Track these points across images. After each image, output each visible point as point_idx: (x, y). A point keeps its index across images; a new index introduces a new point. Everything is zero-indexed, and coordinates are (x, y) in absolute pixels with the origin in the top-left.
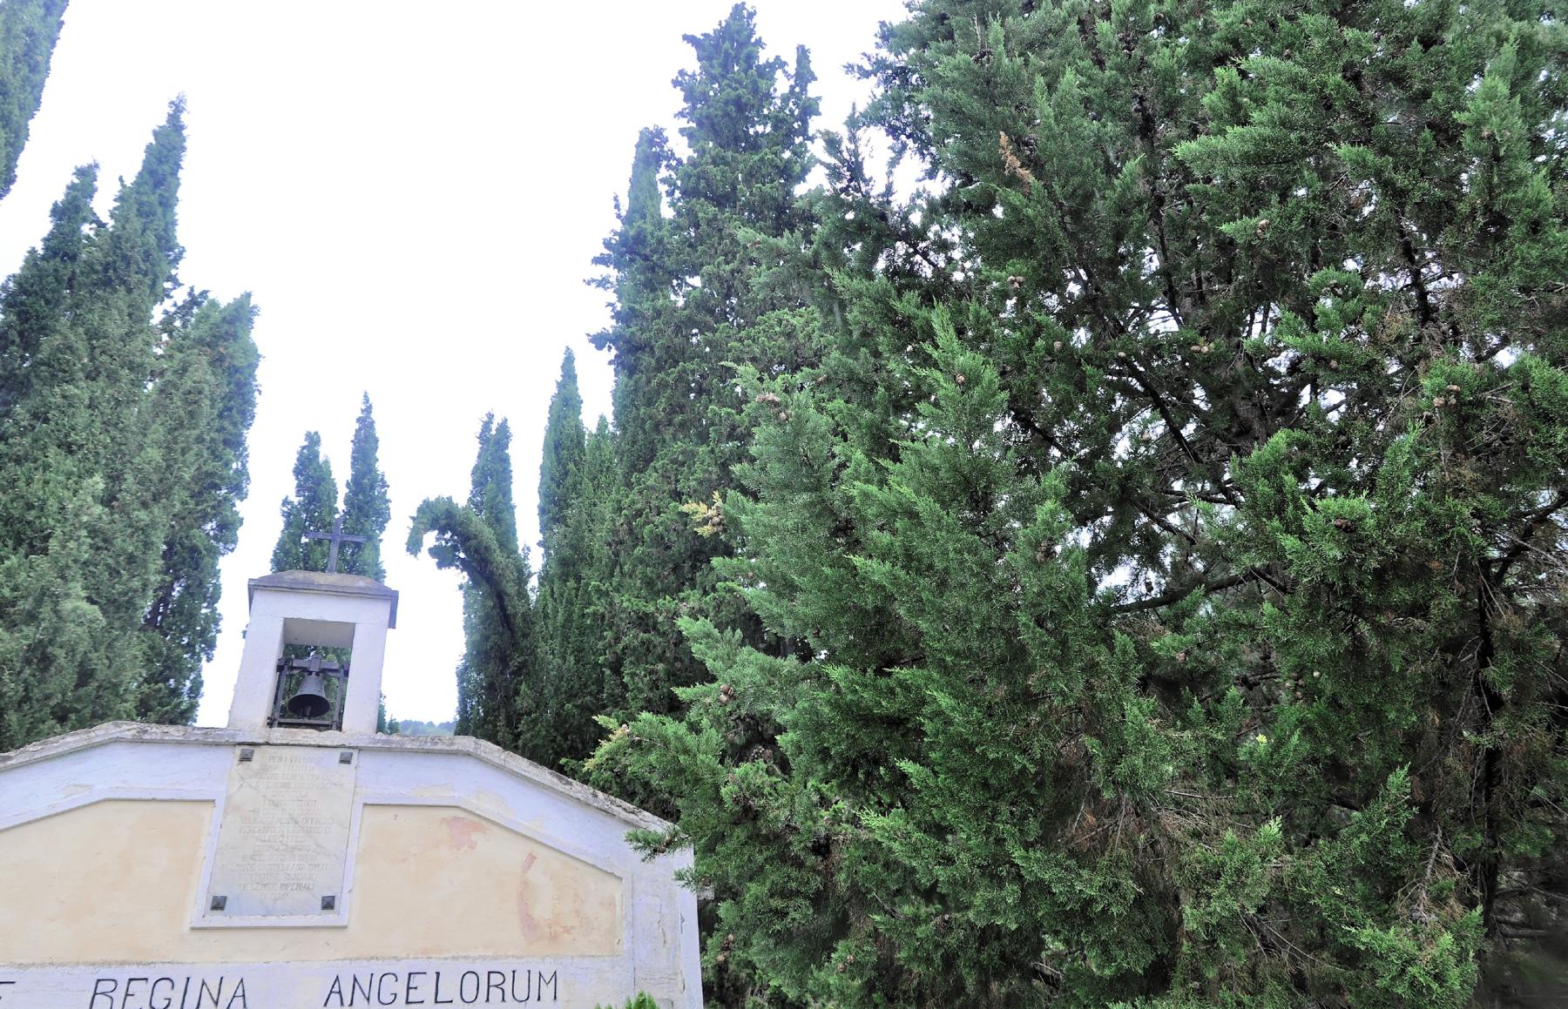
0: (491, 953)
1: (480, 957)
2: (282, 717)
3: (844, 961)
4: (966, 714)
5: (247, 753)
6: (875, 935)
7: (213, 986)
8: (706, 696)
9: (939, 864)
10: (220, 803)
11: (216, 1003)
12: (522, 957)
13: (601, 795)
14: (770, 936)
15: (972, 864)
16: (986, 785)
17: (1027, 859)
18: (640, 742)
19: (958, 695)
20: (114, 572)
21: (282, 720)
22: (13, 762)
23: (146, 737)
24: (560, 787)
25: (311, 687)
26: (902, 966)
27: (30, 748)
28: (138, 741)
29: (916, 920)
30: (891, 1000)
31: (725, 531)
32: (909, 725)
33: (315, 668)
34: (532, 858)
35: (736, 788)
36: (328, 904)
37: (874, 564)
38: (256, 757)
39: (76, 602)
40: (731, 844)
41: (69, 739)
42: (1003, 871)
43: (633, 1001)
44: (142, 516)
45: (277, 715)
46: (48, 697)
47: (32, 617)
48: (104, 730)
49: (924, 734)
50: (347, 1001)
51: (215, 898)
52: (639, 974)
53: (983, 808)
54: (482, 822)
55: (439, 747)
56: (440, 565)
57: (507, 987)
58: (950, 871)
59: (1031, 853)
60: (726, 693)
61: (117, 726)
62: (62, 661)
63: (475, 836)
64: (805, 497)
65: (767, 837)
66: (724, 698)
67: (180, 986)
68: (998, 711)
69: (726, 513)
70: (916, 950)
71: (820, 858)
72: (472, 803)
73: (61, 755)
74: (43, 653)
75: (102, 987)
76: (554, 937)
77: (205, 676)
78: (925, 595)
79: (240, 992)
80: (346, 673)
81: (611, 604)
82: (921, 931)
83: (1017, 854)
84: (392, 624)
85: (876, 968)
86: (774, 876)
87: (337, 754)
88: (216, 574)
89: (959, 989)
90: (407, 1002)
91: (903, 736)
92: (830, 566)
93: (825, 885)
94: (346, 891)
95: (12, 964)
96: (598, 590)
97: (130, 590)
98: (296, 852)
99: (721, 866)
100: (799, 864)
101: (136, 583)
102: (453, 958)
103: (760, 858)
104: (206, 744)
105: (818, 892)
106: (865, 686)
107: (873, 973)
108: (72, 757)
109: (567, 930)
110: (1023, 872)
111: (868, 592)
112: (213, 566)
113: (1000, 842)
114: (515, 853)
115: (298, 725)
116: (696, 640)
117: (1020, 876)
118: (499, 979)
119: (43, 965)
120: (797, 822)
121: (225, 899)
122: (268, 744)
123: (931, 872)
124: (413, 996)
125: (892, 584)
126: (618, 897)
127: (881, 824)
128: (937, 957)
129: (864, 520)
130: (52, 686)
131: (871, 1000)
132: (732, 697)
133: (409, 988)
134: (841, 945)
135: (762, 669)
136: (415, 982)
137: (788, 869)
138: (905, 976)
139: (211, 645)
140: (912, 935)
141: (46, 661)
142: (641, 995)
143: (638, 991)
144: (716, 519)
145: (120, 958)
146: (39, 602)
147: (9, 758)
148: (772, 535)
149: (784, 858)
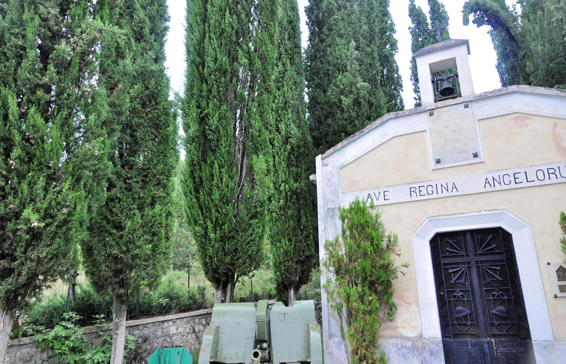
1: (542, 164)
10: (428, 130)
11: (448, 191)
12: (561, 162)
20: (367, 71)
21: (439, 99)
22: (365, 132)
23: (398, 116)
24: (562, 94)
25: (446, 85)
27: (368, 127)
28: (396, 118)
33: (445, 78)
34: (556, 125)
38: (434, 113)
39: (361, 83)
41: (377, 122)
44: (369, 49)
46: (363, 114)
47: (351, 92)
48: (386, 116)
50: (492, 185)
51: (436, 160)
54: (529, 116)
55: (502, 92)
56: (478, 26)
57: (557, 173)
61: (389, 114)
62: (363, 102)
63: (527, 122)
72: (523, 110)
75: (412, 190)
77: (403, 97)
79: (454, 187)
80: (457, 76)
84: (469, 53)
87: (463, 105)
88: (395, 62)
90: (516, 183)
94: (481, 152)
95: (386, 186)
96: (557, 9)
97: (373, 75)
101: (375, 72)
102: (530, 166)
104: (417, 113)
108: (380, 127)
112: (393, 59)
114: (547, 125)
115: (447, 99)
118: (553, 171)
119: (393, 186)
124: (517, 181)
130: (364, 110)
133: (515, 178)
141: (359, 103)
146: (351, 87)
147: (364, 131)
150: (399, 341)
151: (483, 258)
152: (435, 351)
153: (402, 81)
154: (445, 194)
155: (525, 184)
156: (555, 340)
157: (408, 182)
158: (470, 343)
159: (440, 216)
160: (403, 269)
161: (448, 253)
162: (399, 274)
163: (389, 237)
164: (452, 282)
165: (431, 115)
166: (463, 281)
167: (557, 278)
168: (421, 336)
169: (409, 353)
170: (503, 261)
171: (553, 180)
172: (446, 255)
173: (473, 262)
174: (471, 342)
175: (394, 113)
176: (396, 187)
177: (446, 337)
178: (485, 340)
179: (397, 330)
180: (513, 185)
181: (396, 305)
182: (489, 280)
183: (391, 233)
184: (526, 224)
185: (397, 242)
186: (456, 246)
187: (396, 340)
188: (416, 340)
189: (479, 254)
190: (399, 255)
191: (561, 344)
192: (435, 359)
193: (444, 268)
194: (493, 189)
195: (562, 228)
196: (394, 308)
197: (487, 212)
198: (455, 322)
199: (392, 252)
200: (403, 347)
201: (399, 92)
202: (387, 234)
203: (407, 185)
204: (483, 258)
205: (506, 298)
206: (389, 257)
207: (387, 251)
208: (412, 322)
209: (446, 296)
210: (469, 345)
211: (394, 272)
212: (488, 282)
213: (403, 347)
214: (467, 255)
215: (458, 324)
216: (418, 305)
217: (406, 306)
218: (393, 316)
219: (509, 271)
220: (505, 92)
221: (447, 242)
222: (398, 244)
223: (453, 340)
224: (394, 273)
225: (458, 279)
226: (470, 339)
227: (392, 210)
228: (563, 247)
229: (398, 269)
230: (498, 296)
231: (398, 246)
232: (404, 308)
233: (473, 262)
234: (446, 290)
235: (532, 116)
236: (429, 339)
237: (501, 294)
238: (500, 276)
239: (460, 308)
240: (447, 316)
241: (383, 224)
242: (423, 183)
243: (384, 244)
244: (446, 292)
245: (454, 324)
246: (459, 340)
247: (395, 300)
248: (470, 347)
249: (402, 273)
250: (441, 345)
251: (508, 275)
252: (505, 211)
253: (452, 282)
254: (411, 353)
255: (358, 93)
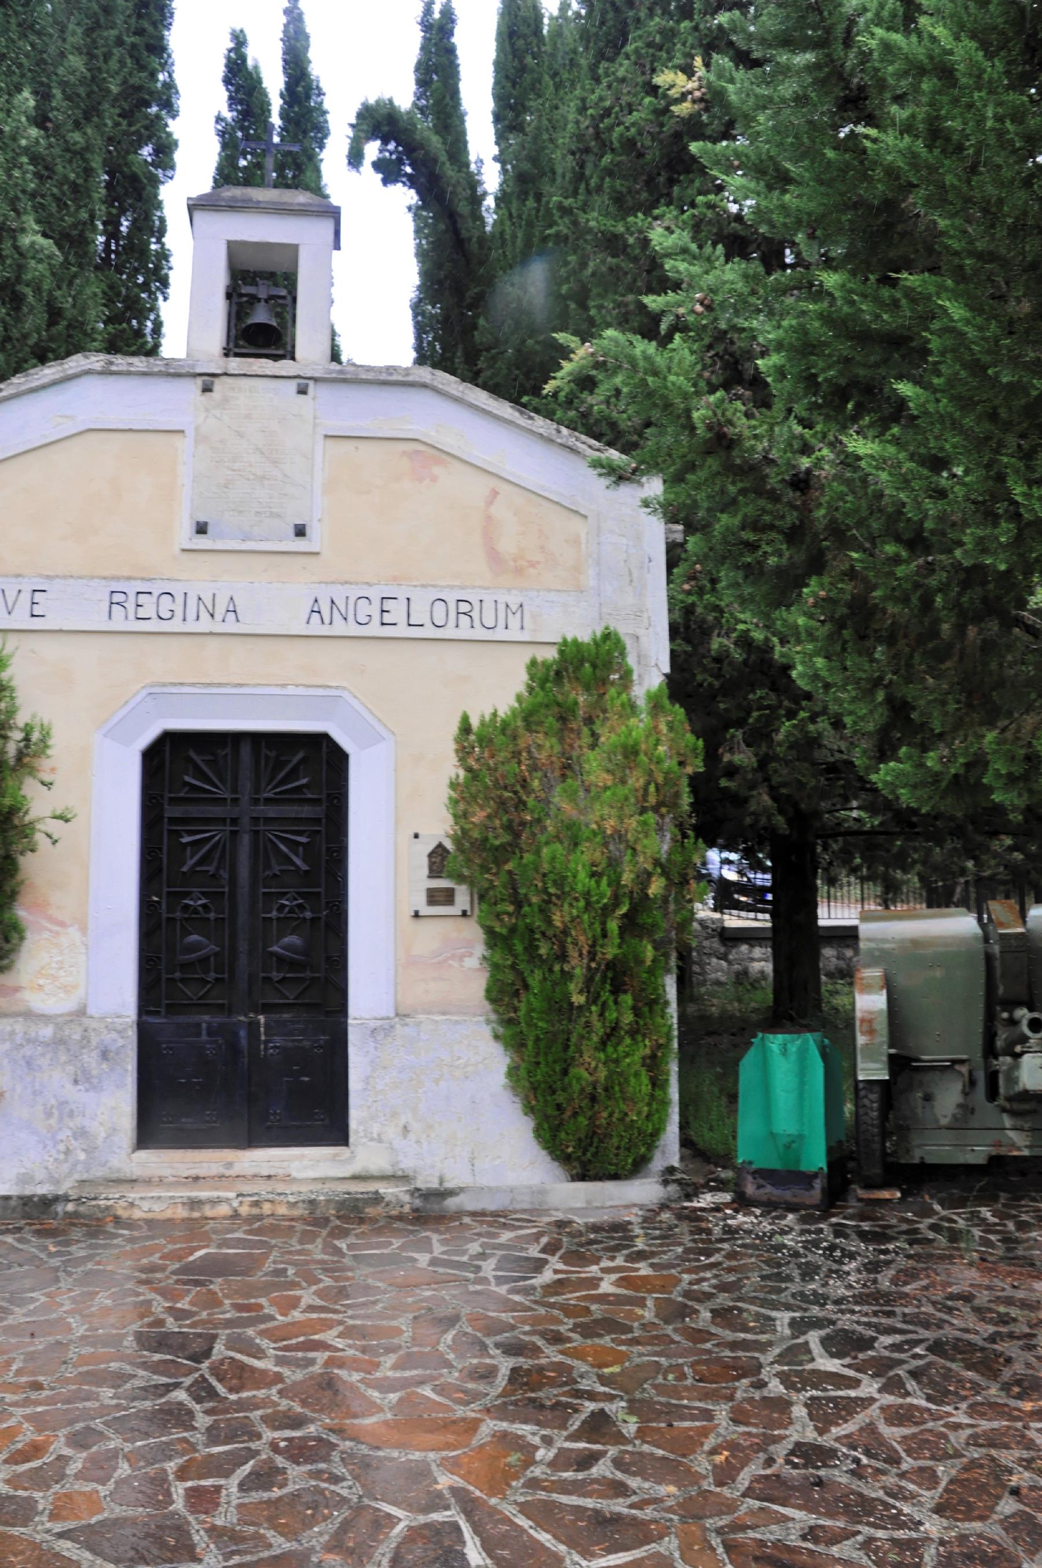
0: (457, 583)
2: (237, 346)
3: (814, 594)
4: (981, 329)
5: (208, 383)
6: (851, 574)
7: (208, 600)
8: (680, 306)
9: (930, 497)
10: (190, 433)
11: (212, 616)
13: (565, 431)
14: (738, 568)
15: (967, 499)
16: (993, 416)
17: (1027, 496)
18: (605, 363)
19: (975, 307)
20: (61, 205)
21: (237, 350)
23: (114, 368)
24: (522, 421)
25: (261, 316)
26: (876, 605)
27: (15, 380)
29: (896, 560)
30: (863, 637)
31: (707, 110)
32: (914, 344)
33: (263, 295)
34: (495, 493)
35: (710, 413)
36: (300, 531)
37: (890, 138)
39: (32, 238)
40: (702, 474)
42: (1001, 508)
43: (599, 634)
45: (231, 345)
46: (25, 336)
48: (76, 363)
49: (929, 352)
50: (327, 620)
51: (198, 523)
52: (605, 610)
53: (988, 438)
55: (395, 377)
56: (386, 182)
57: (475, 614)
58: (941, 504)
59: (1035, 490)
60: (702, 304)
61: (86, 357)
62: (31, 299)
63: (436, 470)
64: (807, 57)
65: (740, 467)
66: (699, 308)
67: (180, 599)
68: (1019, 328)
69: (709, 85)
70: (894, 589)
71: (798, 494)
72: (432, 435)
73: (44, 387)
74: (14, 292)
76: (519, 571)
78: (949, 179)
80: (294, 300)
81: (575, 223)
82: (901, 571)
83: (1018, 491)
84: (337, 246)
85: (850, 605)
86: (749, 508)
87: (292, 386)
88: (159, 206)
89: (934, 633)
91: (903, 357)
92: (835, 149)
93: (801, 521)
95: (41, 576)
96: (560, 207)
98: (266, 482)
99: (689, 495)
100: (774, 497)
101: (84, 215)
102: (423, 586)
103: (732, 489)
105: (793, 527)
106: (864, 296)
107: (845, 610)
109: (533, 564)
110: (1022, 510)
111: (879, 181)
112: (156, 195)
113: (1001, 478)
114: (481, 486)
116: (668, 255)
117: (1019, 515)
119: (65, 577)
120: (774, 454)
121: (206, 524)
122: (226, 374)
123: (919, 504)
124: (387, 618)
125: (909, 164)
126: (583, 535)
127: (870, 452)
128: (915, 600)
129: (882, 85)
131: (840, 634)
132: (709, 308)
134: (813, 581)
135: (745, 276)
136: (388, 605)
137: (762, 502)
138: (878, 616)
139: (165, 283)
140: (891, 574)
142: (607, 628)
143: (603, 625)
144: (697, 94)
145: (126, 574)
148: (765, 108)
149: (760, 490)
150: (19, 1026)
151: (272, 811)
152: (113, 1048)
153: (170, 268)
154: (205, 624)
155: (402, 630)
156: (397, 1015)
157: (106, 573)
158: (208, 1028)
159: (182, 684)
160: (55, 827)
161: (186, 789)
162: (39, 838)
163: (28, 730)
164: (185, 869)
165: (207, 389)
166: (211, 869)
167: (425, 871)
168: (81, 1012)
169: (43, 1055)
170: (317, 821)
171: (464, 633)
172: (182, 795)
173: (245, 821)
174: (209, 1024)
175: (103, 357)
176: (71, 581)
177: (149, 1013)
178: (242, 1018)
179: (18, 995)
180: (374, 629)
181: (24, 924)
182: (276, 869)
183: (34, 716)
184: (385, 733)
185: (47, 747)
186: (211, 774)
187: (11, 1020)
188: (67, 1022)
189: (268, 801)
190: (48, 785)
191: (406, 1025)
192: (112, 1070)
193: (169, 831)
194: (325, 630)
195: (457, 751)
196: (15, 936)
197: (301, 691)
198: (178, 975)
199: (30, 774)
200: (29, 1041)
201: (156, 299)
202: (21, 719)
203: (103, 582)
204: (272, 811)
205: (308, 914)
206: (20, 789)
207: (14, 770)
208: (62, 973)
209: (164, 906)
210: (204, 1032)
211: (26, 831)
212: (275, 875)
213: (29, 1041)
214: (235, 801)
215: (182, 980)
216: (84, 930)
217: (50, 931)
218: (12, 956)
219: (328, 849)
220: (400, 378)
221: (190, 760)
222: (49, 752)
223: (164, 1020)
224: (26, 837)
225: (200, 863)
226: (207, 1018)
227: (51, 649)
228: (450, 798)
229: (38, 826)
230: (291, 911)
231: (48, 757)
232: (46, 935)
233: (245, 821)
234: (166, 889)
235: (448, 459)
236: (102, 1019)
237: (300, 906)
238: (304, 860)
239: (194, 938)
240: (159, 958)
241: (12, 690)
242: (149, 584)
243: (11, 749)
244: (164, 896)
245: (173, 980)
246: (181, 1019)
247: (22, 912)
248: (204, 1037)
249: (49, 836)
250: (132, 1034)
251: (324, 858)
252: (345, 694)
253: (185, 869)
254: (48, 1056)
255: (21, 268)
